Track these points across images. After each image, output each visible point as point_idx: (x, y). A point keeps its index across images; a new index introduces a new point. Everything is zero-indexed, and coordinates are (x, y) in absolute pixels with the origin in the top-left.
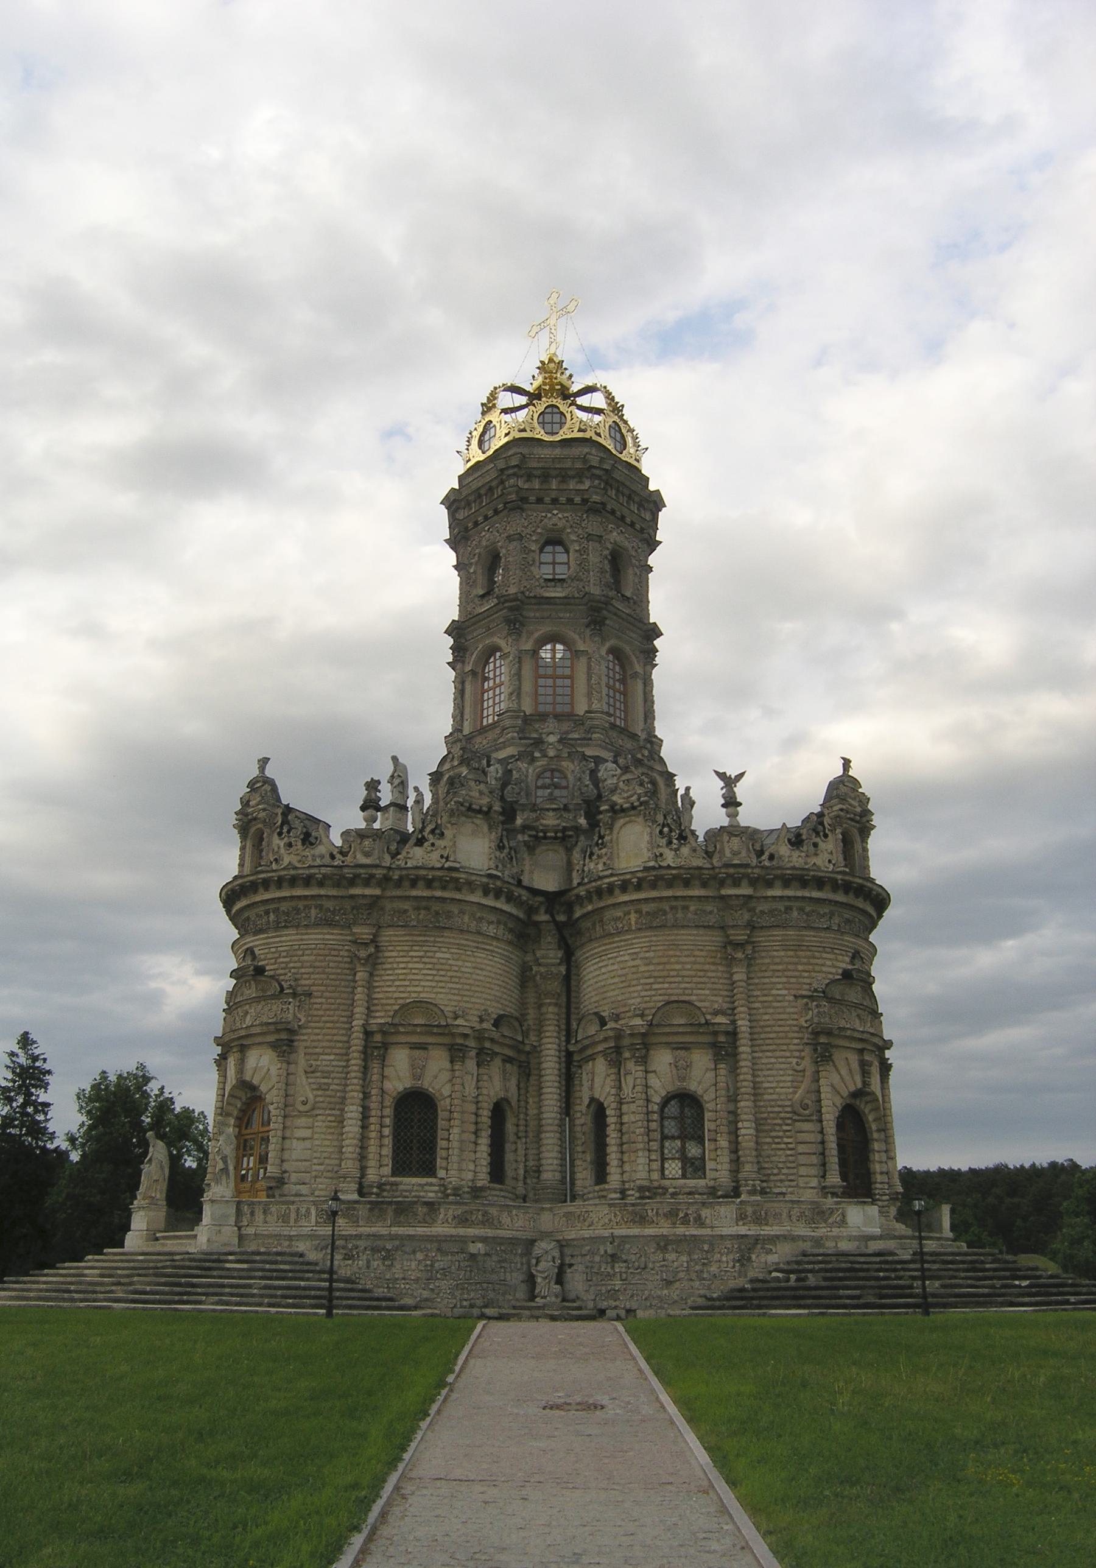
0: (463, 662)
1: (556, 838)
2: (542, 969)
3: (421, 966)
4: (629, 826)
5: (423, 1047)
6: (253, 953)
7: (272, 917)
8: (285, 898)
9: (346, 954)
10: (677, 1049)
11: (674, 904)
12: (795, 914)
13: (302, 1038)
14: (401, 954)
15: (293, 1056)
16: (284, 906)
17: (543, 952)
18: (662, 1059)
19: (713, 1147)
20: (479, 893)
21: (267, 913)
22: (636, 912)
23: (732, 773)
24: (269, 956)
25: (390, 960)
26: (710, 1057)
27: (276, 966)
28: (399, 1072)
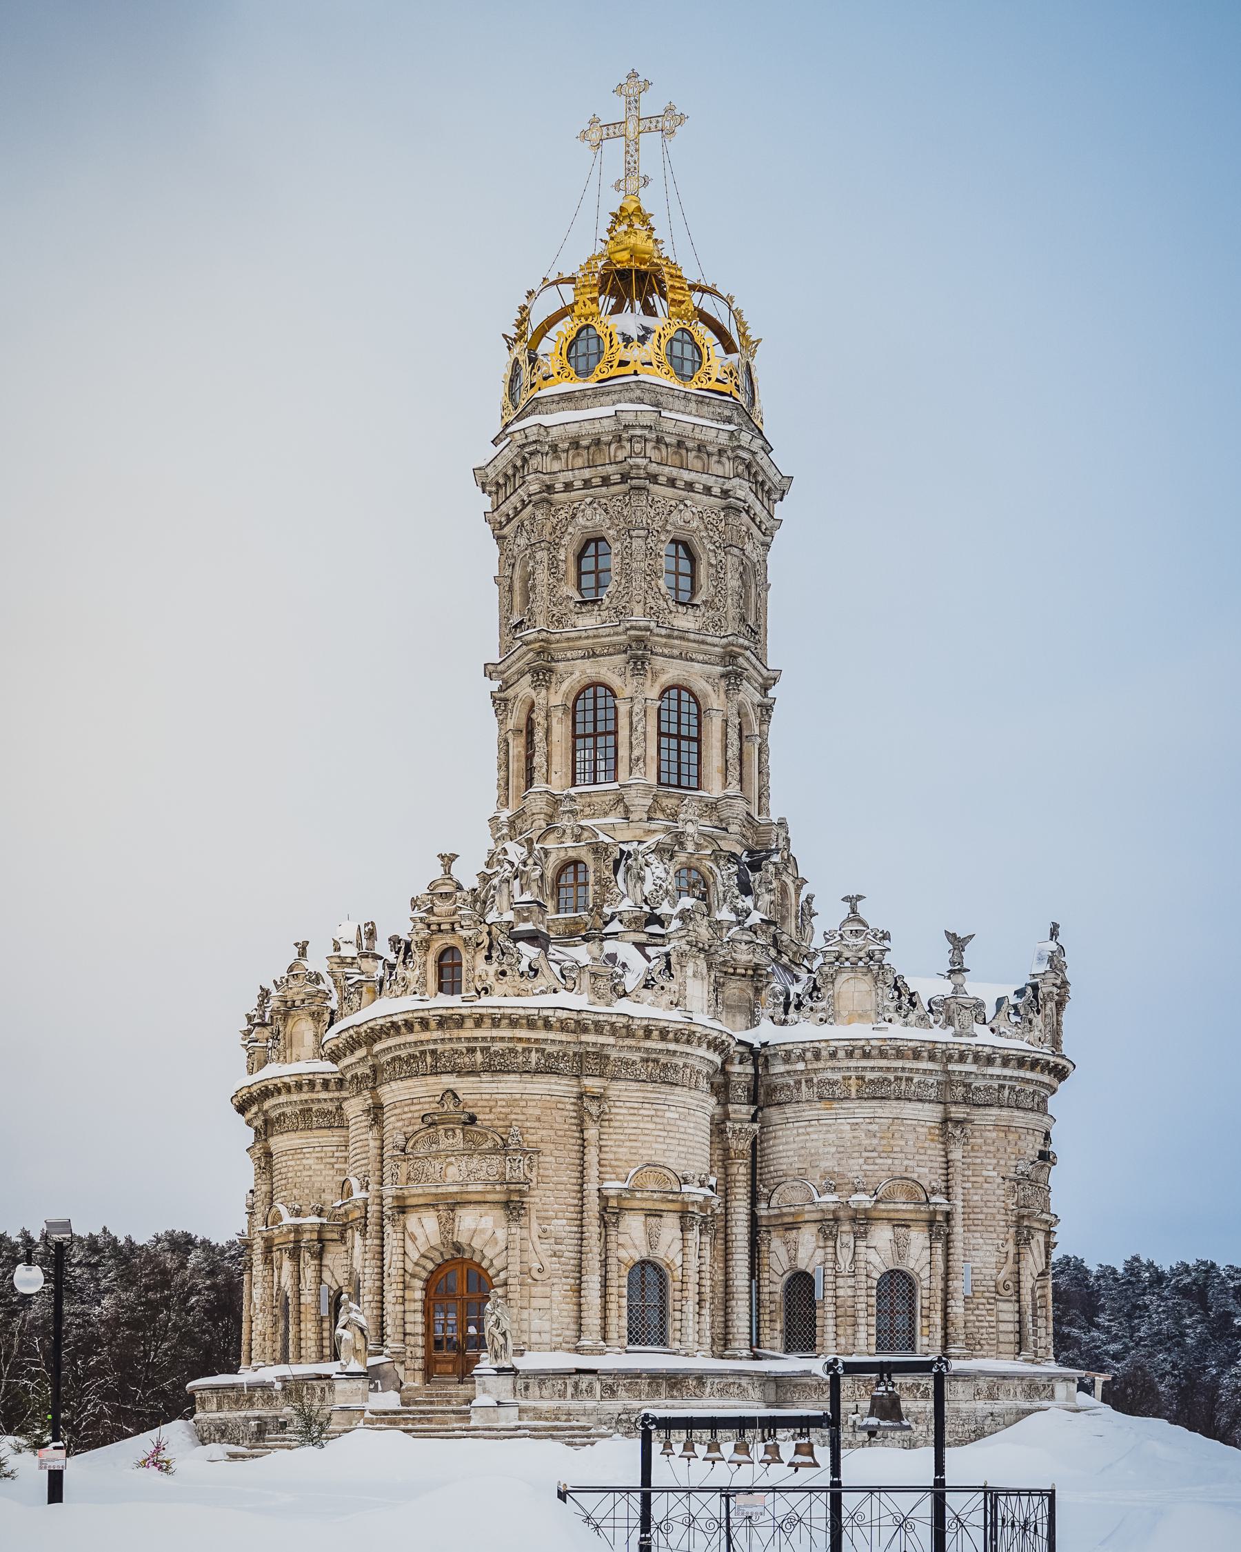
0: (548, 688)
1: (744, 976)
2: (738, 1126)
3: (652, 1126)
4: (852, 982)
5: (657, 1214)
6: (456, 1096)
7: (479, 1057)
8: (502, 1039)
9: (572, 1107)
10: (898, 1225)
11: (900, 1074)
12: (1007, 1092)
13: (532, 1200)
14: (632, 1111)
15: (524, 1220)
16: (497, 1046)
17: (737, 1107)
18: (882, 1235)
19: (925, 1324)
20: (705, 1046)
21: (471, 1051)
22: (857, 1078)
23: (961, 935)
24: (480, 1104)
25: (618, 1117)
26: (927, 1235)
27: (492, 1116)
28: (633, 1240)
